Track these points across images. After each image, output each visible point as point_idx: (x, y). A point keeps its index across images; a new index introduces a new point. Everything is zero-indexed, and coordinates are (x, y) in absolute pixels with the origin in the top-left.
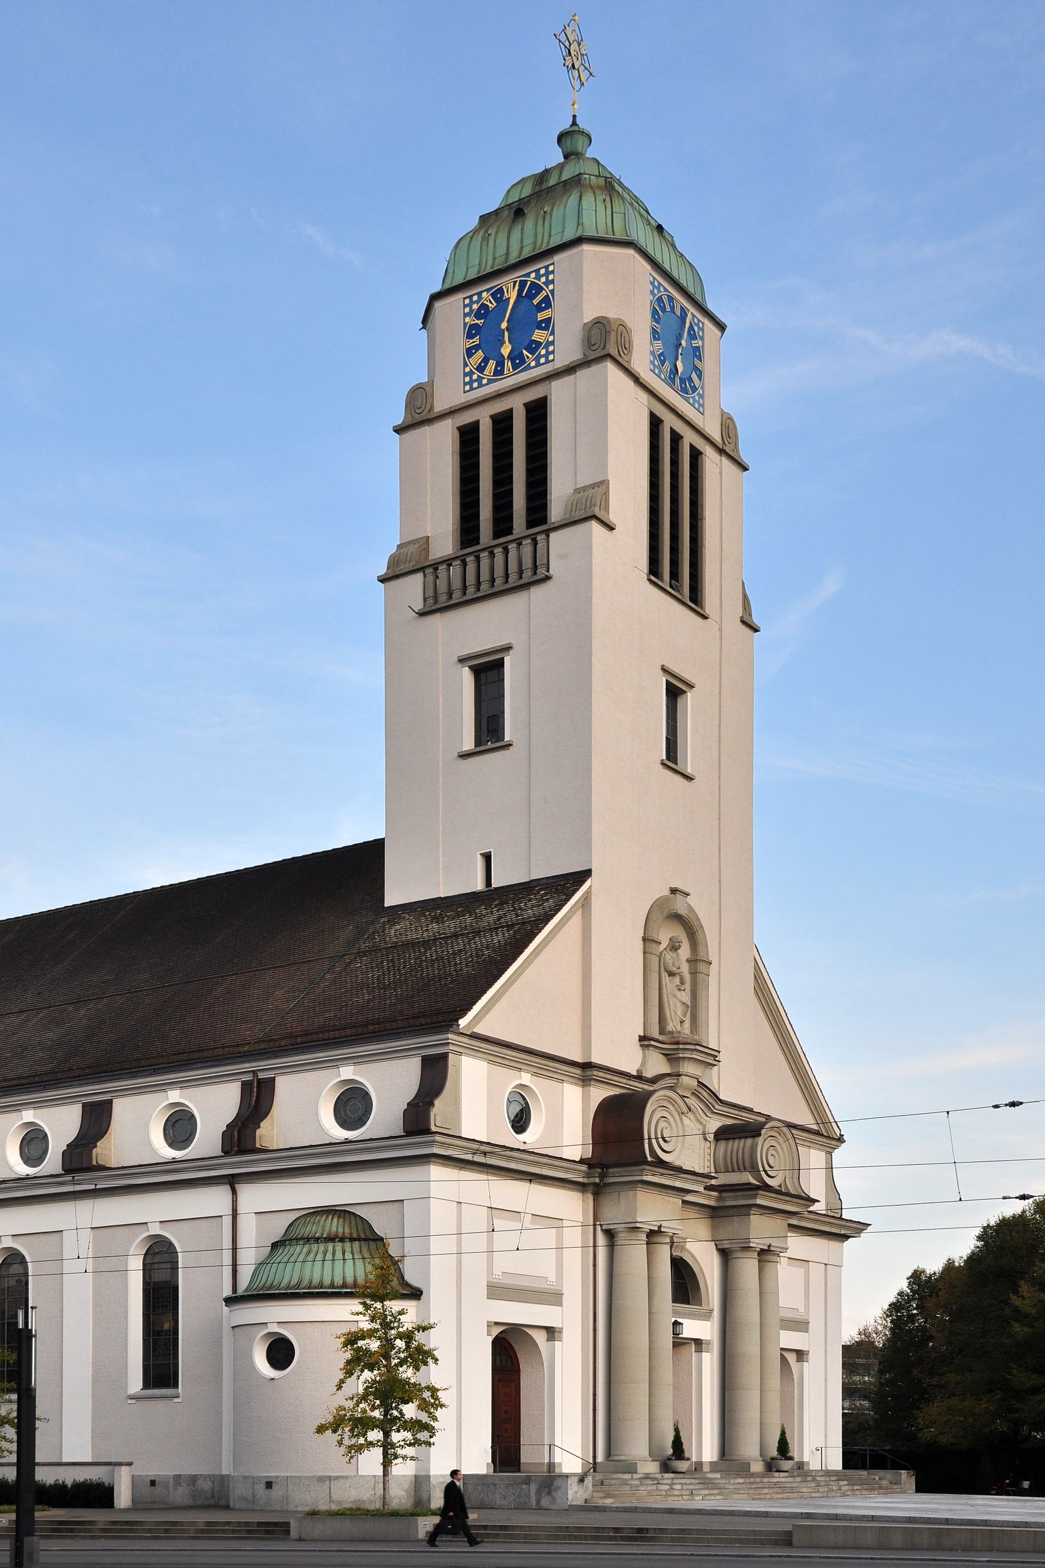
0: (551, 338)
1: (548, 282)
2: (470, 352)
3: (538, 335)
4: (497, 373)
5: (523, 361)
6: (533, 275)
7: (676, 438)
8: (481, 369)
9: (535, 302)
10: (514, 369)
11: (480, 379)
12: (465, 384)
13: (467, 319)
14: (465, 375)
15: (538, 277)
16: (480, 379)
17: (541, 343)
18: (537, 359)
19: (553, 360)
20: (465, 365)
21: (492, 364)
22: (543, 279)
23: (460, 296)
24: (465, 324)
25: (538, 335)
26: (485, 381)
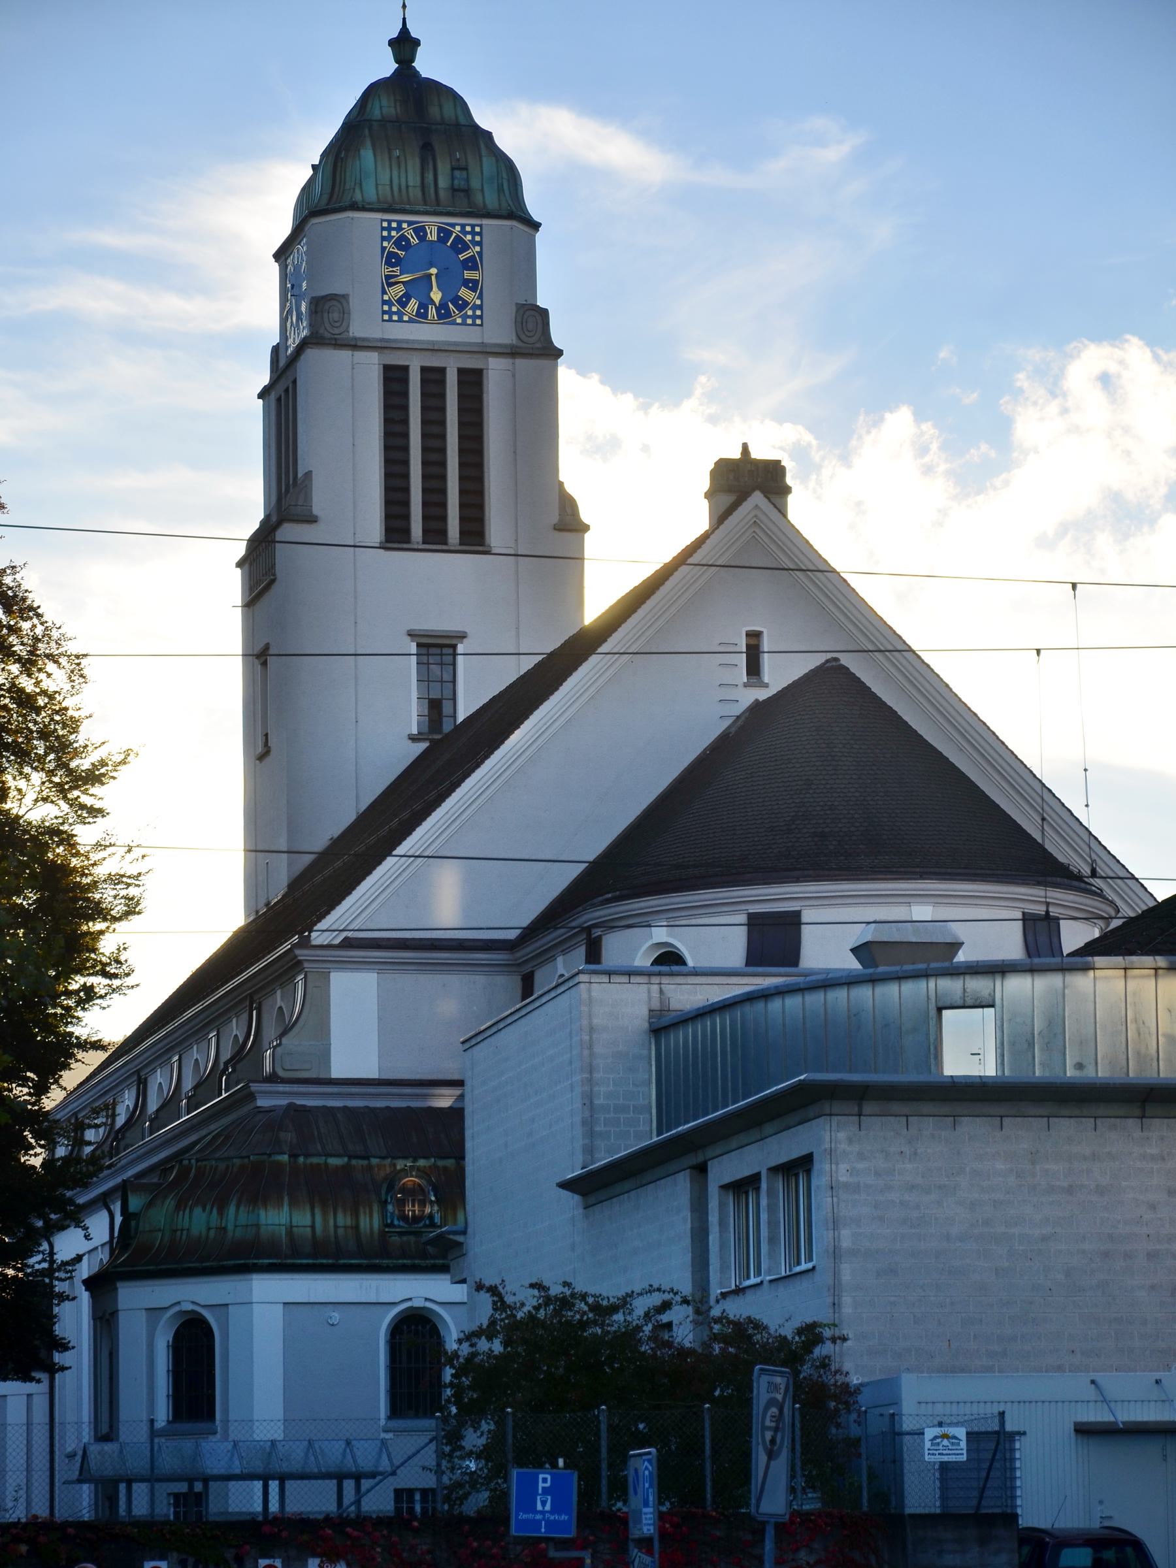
2: (390, 281)
3: (464, 293)
5: (448, 314)
6: (458, 228)
9: (462, 257)
11: (398, 313)
17: (468, 304)
18: (465, 317)
19: (481, 325)
20: (384, 292)
21: (413, 305)
22: (469, 237)
23: (379, 216)
24: (384, 249)
25: (464, 293)
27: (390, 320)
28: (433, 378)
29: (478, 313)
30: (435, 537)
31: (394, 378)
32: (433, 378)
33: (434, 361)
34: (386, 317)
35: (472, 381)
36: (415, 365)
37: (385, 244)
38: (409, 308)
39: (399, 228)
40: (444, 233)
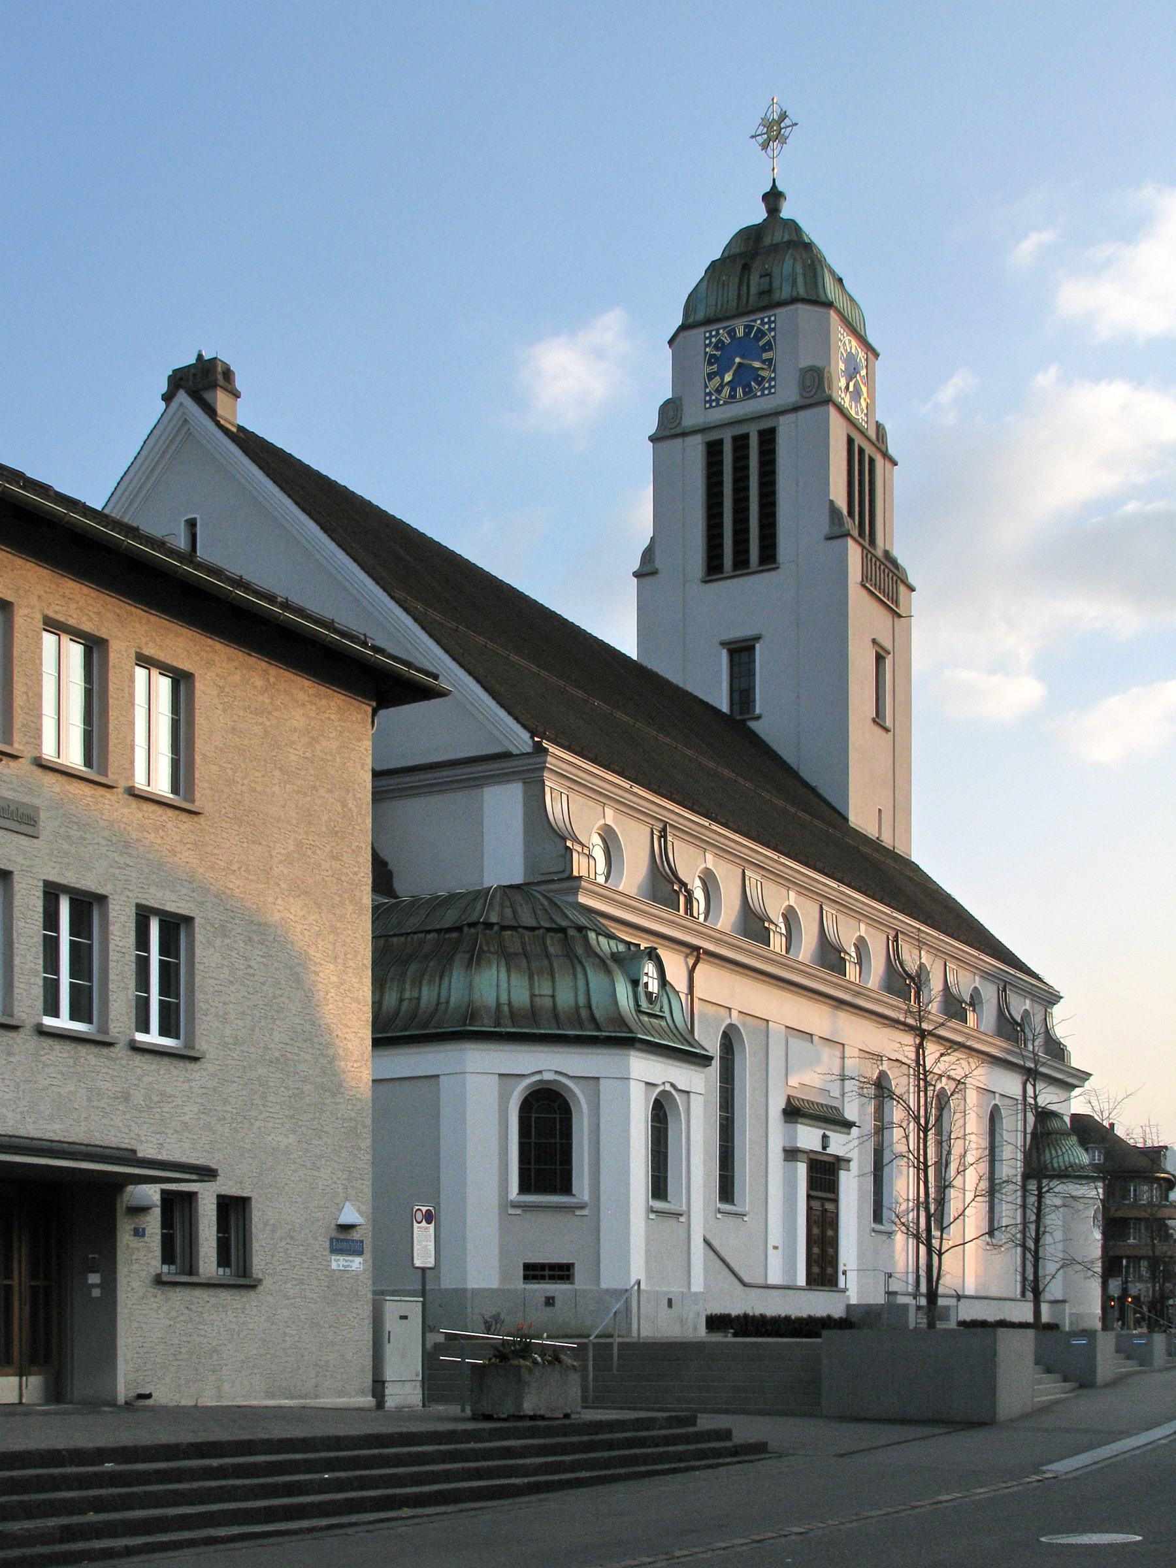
0: (773, 375)
1: (770, 330)
4: (731, 397)
6: (759, 322)
7: (861, 451)
8: (719, 391)
9: (761, 343)
10: (744, 395)
11: (717, 400)
12: (706, 402)
13: (708, 349)
14: (707, 394)
15: (763, 323)
16: (717, 400)
18: (763, 390)
22: (767, 326)
23: (702, 329)
24: (706, 353)
26: (721, 402)
27: (711, 407)
28: (741, 443)
29: (773, 383)
30: (741, 563)
31: (713, 450)
32: (741, 443)
33: (739, 430)
34: (708, 405)
35: (768, 438)
36: (727, 436)
37: (708, 349)
38: (723, 394)
39: (718, 333)
40: (748, 328)
